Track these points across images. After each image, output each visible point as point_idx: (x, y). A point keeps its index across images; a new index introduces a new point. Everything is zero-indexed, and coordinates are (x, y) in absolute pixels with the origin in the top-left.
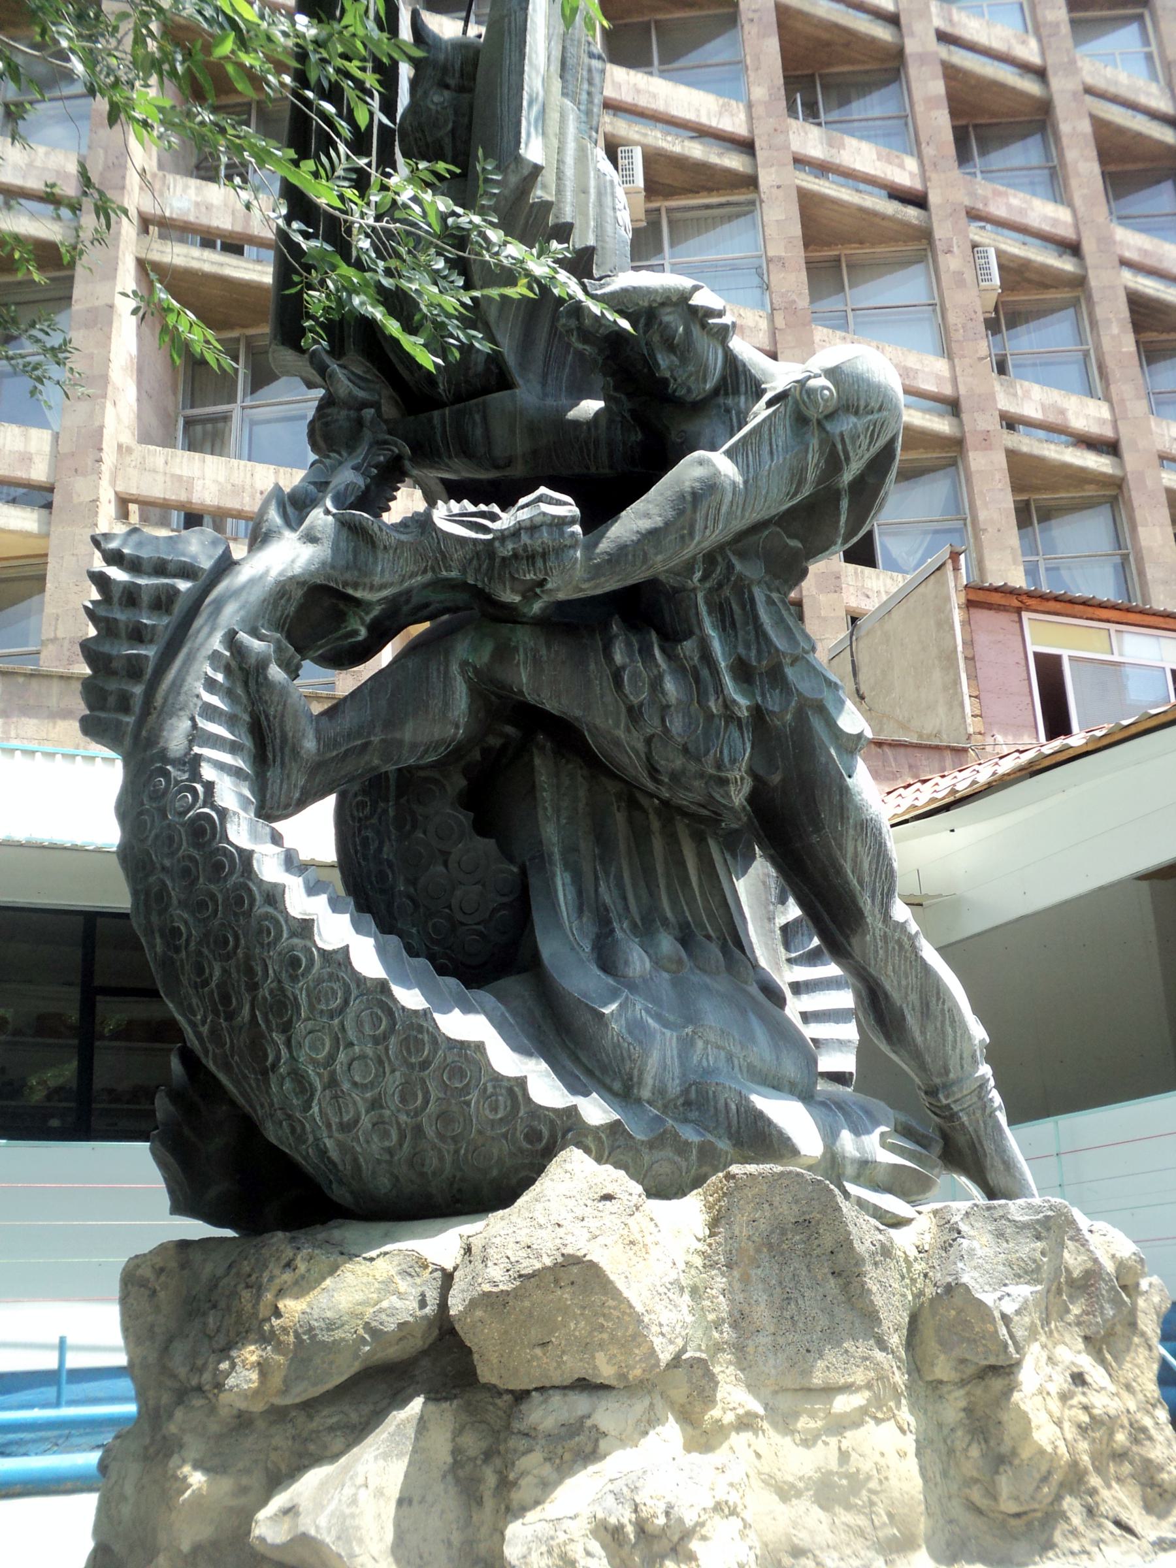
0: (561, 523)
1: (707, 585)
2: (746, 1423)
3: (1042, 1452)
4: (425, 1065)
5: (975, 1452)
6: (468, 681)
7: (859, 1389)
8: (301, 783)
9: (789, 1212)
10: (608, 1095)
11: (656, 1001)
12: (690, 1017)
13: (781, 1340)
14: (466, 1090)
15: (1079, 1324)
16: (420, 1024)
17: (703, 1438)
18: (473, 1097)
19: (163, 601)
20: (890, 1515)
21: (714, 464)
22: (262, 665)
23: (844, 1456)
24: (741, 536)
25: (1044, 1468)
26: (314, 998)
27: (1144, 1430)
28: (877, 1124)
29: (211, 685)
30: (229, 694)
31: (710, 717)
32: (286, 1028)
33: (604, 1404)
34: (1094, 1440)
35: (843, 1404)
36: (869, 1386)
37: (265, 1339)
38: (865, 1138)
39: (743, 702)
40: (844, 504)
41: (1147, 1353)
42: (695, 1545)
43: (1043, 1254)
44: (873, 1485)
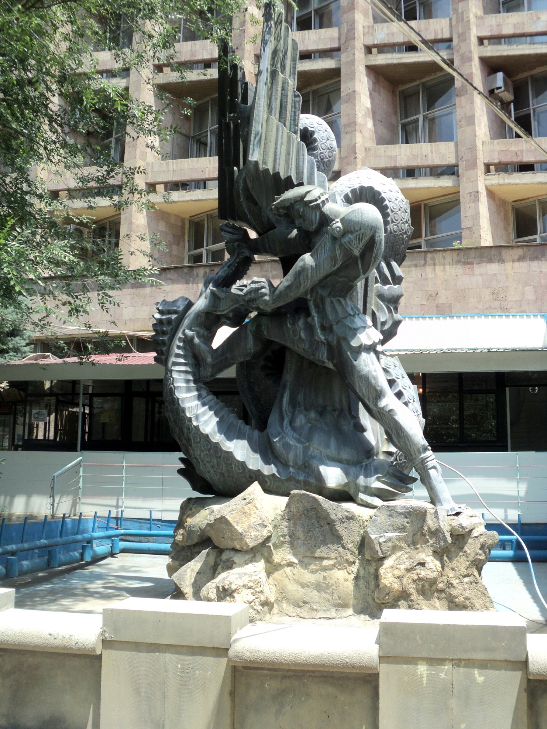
0: (257, 290)
1: (313, 299)
2: (290, 564)
3: (386, 586)
4: (220, 457)
5: (373, 583)
6: (253, 335)
7: (332, 559)
8: (210, 370)
9: (308, 506)
10: (279, 464)
11: (300, 435)
12: (309, 439)
13: (306, 542)
14: (231, 464)
15: (432, 546)
16: (216, 447)
17: (272, 568)
18: (233, 466)
19: (169, 321)
20: (339, 597)
21: (307, 259)
22: (192, 339)
23: (325, 578)
24: (321, 281)
25: (387, 591)
26: (194, 438)
27: (452, 584)
28: (376, 473)
29: (179, 347)
30: (184, 348)
31: (318, 342)
32: (191, 446)
33: (237, 555)
34: (418, 585)
35: (325, 563)
36: (336, 558)
37: (184, 528)
38: (369, 479)
39: (322, 338)
40: (359, 262)
41: (465, 558)
42: (235, 594)
43: (408, 523)
44: (333, 587)
